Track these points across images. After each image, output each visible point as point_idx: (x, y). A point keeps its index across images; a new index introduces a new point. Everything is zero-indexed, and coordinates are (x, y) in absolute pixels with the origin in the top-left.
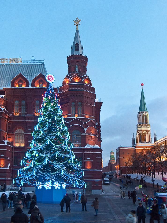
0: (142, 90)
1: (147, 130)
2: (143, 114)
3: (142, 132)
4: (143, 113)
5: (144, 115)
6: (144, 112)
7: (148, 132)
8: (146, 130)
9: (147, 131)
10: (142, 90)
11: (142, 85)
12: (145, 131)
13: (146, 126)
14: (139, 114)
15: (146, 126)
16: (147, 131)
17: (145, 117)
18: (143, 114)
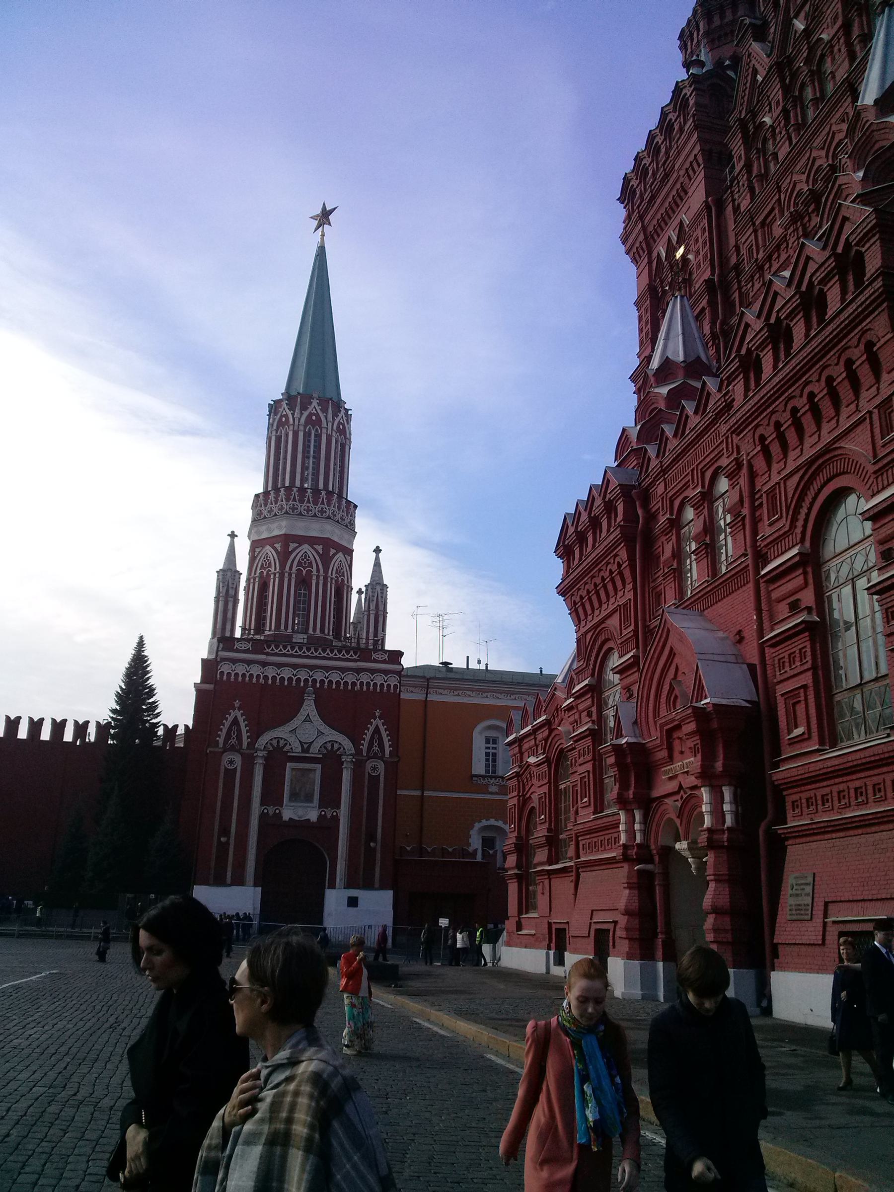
0: (321, 253)
1: (327, 543)
2: (306, 414)
3: (284, 556)
4: (304, 408)
5: (314, 422)
6: (315, 403)
7: (326, 559)
8: (312, 541)
9: (320, 548)
10: (321, 253)
11: (324, 217)
12: (306, 547)
13: (315, 503)
14: (276, 414)
15: (315, 509)
16: (320, 548)
17: (318, 437)
18: (306, 414)
